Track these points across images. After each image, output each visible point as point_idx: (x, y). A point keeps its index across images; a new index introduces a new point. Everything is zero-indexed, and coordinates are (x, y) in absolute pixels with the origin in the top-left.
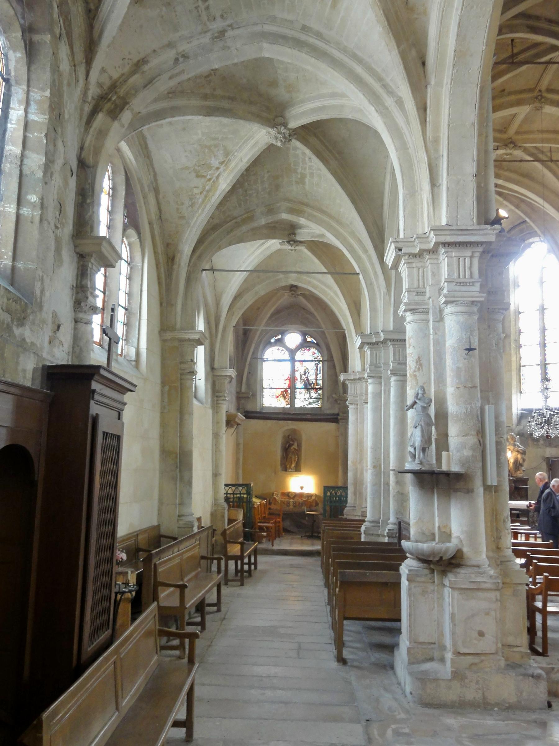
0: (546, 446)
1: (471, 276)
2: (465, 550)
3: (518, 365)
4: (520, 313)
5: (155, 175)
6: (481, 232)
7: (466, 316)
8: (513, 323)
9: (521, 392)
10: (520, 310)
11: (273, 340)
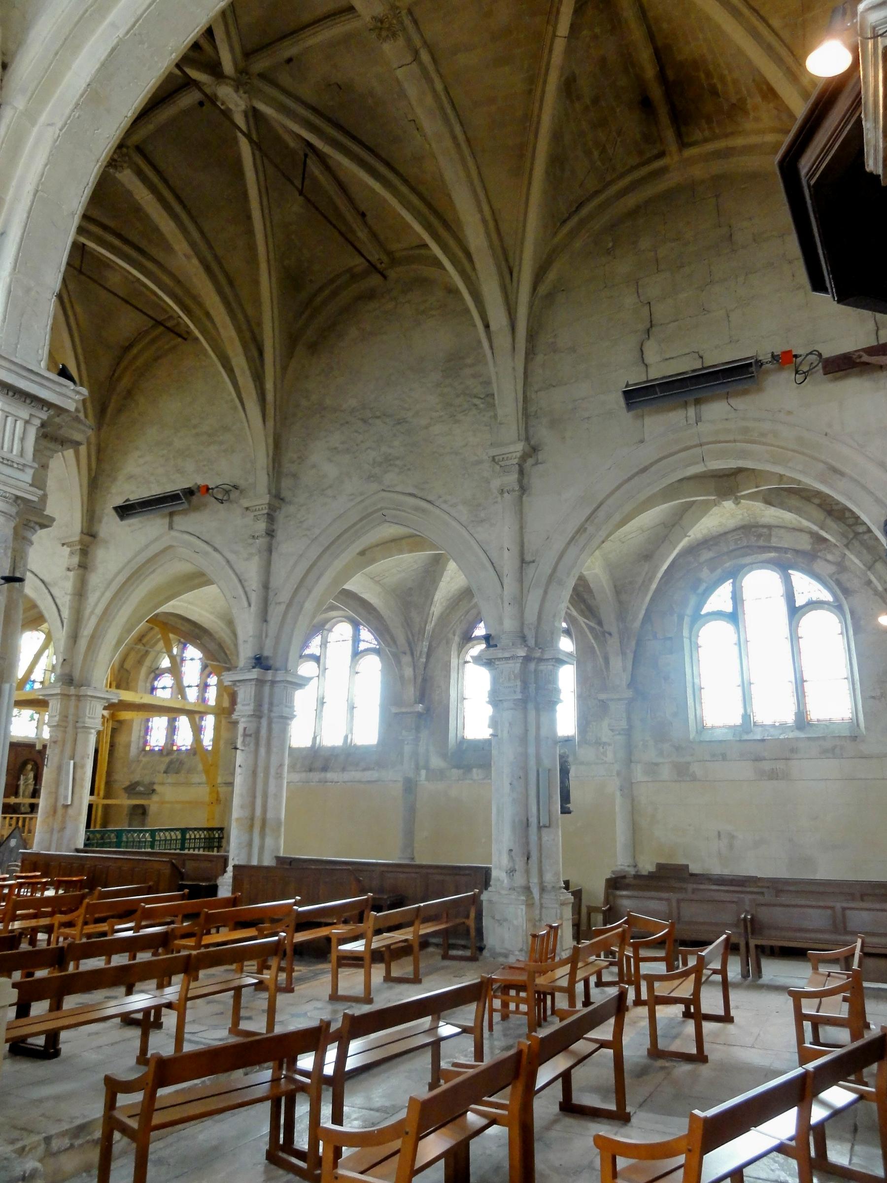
1: (22, 454)
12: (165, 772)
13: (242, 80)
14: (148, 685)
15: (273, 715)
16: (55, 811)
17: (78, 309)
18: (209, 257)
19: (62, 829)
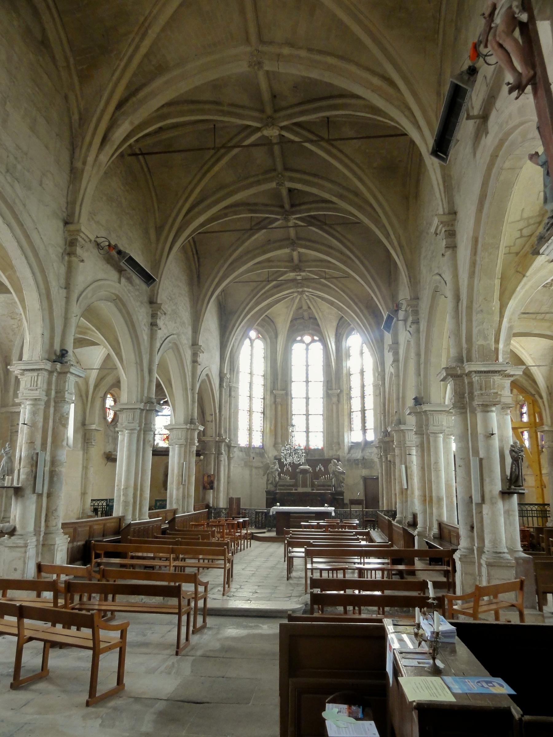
1: (37, 386)
2: (17, 527)
4: (350, 375)
6: (38, 364)
7: (32, 406)
8: (345, 382)
10: (351, 373)
11: (162, 402)
12: (528, 467)
13: (270, 122)
14: (518, 412)
15: (428, 431)
18: (341, 191)
19: (407, 501)
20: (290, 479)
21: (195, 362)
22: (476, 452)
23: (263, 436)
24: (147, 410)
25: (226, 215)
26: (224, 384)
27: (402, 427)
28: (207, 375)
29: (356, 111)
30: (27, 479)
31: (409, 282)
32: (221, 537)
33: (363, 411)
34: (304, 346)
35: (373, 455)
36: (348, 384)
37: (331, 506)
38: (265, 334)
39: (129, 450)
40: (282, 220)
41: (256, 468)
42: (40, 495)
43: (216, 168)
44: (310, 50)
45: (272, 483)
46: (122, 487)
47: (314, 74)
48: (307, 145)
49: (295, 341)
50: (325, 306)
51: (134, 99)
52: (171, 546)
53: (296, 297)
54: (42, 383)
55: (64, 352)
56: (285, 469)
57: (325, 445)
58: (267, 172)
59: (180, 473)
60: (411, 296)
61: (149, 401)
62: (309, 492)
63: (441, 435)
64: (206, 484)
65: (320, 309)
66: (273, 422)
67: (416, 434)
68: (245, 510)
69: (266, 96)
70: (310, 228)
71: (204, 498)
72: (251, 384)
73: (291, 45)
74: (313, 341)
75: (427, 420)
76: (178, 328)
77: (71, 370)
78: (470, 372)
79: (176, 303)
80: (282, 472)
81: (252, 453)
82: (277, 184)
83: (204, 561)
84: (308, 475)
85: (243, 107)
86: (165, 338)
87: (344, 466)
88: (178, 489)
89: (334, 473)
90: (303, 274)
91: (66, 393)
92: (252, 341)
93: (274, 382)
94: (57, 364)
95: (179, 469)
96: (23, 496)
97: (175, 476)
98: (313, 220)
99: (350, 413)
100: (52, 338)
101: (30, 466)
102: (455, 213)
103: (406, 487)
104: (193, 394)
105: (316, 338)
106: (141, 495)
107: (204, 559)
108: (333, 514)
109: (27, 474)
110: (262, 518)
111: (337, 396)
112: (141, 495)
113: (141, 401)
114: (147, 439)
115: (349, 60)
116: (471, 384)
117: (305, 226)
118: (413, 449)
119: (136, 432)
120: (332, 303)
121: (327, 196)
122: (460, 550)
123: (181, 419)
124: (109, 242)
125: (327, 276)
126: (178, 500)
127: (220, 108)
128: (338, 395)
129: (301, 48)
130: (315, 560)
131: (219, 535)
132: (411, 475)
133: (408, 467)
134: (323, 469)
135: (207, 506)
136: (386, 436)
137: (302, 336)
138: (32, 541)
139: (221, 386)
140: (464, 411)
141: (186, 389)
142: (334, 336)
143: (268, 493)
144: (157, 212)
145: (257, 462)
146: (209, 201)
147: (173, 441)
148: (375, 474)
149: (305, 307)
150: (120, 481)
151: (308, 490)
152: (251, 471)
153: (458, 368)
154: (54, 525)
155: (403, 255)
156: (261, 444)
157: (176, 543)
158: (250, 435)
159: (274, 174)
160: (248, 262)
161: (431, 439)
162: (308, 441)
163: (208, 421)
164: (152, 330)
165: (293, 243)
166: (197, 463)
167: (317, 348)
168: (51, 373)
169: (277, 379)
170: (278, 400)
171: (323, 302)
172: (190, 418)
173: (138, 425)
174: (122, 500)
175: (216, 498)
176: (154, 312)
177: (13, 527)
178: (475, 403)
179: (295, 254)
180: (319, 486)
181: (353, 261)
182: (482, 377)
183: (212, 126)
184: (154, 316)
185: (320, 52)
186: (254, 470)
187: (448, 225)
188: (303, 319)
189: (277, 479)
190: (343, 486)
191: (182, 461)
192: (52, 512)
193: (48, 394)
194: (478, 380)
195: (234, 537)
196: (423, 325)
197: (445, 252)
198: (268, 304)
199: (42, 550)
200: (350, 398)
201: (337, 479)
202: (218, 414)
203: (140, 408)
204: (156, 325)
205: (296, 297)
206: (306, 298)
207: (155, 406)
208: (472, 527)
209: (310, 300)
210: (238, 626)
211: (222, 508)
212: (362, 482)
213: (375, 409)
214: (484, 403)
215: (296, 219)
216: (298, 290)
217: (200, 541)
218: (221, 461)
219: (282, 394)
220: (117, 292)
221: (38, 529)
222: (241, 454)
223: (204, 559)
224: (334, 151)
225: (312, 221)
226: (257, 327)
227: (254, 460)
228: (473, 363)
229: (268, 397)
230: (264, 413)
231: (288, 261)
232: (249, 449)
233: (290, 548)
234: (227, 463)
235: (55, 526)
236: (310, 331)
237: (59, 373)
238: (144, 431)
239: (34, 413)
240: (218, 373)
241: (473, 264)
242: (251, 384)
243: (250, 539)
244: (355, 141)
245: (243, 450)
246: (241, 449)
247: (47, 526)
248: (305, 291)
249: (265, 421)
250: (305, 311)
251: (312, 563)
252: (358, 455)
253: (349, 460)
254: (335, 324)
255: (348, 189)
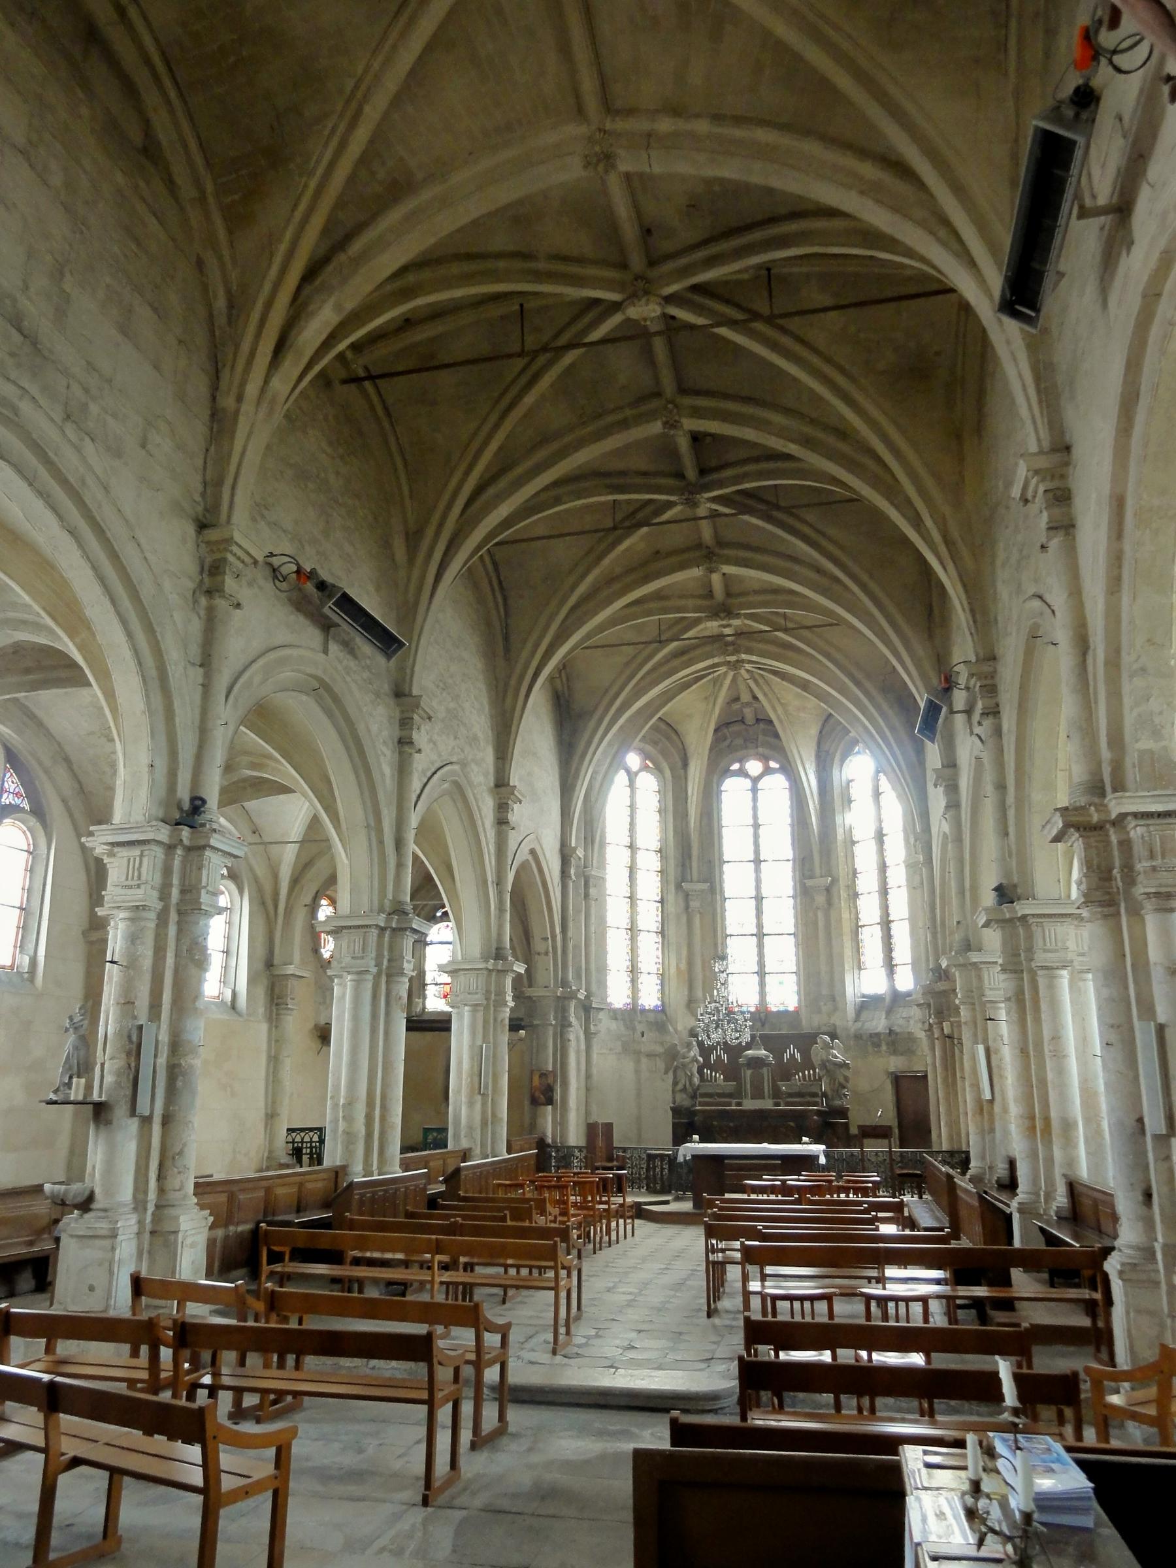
0: (891, 1054)
1: (139, 878)
2: (97, 1191)
3: (853, 925)
4: (854, 843)
5: (59, 744)
6: (141, 830)
7: (128, 923)
8: (841, 859)
9: (860, 968)
11: (439, 914)
13: (640, 287)
15: (1033, 965)
16: (982, 1110)
17: (832, 531)
18: (808, 430)
19: (992, 1130)
20: (725, 1080)
21: (502, 822)
22: (1148, 1010)
23: (662, 985)
24: (394, 930)
25: (558, 501)
26: (572, 871)
27: (975, 957)
28: (533, 852)
29: (826, 245)
30: (118, 1084)
31: (971, 623)
32: (562, 1214)
33: (886, 924)
34: (748, 783)
35: (912, 1022)
36: (850, 865)
37: (817, 1141)
38: (661, 758)
39: (355, 1018)
40: (682, 504)
41: (650, 1055)
42: (146, 1121)
43: (529, 399)
44: (717, 118)
45: (684, 1090)
46: (342, 1101)
47: (730, 170)
48: (723, 331)
49: (727, 773)
50: (789, 693)
51: (342, 257)
52: (434, 1237)
53: (725, 674)
54: (151, 873)
55: (198, 803)
56: (713, 1057)
57: (803, 1004)
58: (641, 399)
59: (476, 1069)
60: (977, 656)
61: (398, 910)
62: (771, 1110)
63: (1065, 973)
64: (537, 1094)
65: (778, 699)
66: (684, 953)
67: (1004, 970)
68: (625, 1150)
69: (630, 232)
70: (746, 517)
71: (533, 1126)
72: (632, 869)
73: (676, 111)
74: (767, 771)
75: (1030, 937)
76: (462, 751)
77: (213, 842)
78: (1123, 816)
79: (458, 696)
80: (707, 1064)
81: (640, 1022)
82: (665, 424)
83: (518, 1272)
84: (765, 1070)
85: (580, 261)
86: (433, 770)
87: (846, 1050)
88: (471, 1104)
89: (823, 1065)
90: (736, 622)
91: (203, 892)
92: (632, 776)
93: (683, 865)
94: (182, 830)
95: (472, 1058)
96: (108, 1123)
97: (464, 1076)
98: (750, 502)
99: (857, 928)
100: (172, 774)
101: (124, 1056)
102: (1068, 449)
103: (988, 1096)
104: (500, 893)
105: (773, 765)
106: (383, 1119)
107: (518, 1267)
108: (823, 1160)
109: (118, 1074)
110: (662, 1169)
111: (825, 893)
112: (383, 1119)
113: (381, 910)
114: (394, 993)
115: (807, 132)
116: (1126, 845)
117: (732, 515)
118: (1000, 1008)
119: (370, 977)
120: (805, 686)
121: (775, 443)
122: (1120, 1250)
123: (476, 950)
124: (298, 564)
125: (790, 625)
126: (470, 1128)
127: (533, 265)
128: (828, 890)
129: (698, 116)
130: (769, 1270)
131: (556, 1211)
132: (999, 1067)
133: (992, 1049)
134: (798, 1056)
135: (541, 1144)
136: (940, 979)
137: (741, 761)
138: (128, 1225)
139: (564, 874)
140: (1112, 910)
141: (485, 882)
142: (813, 758)
143: (676, 1111)
144: (407, 501)
145: (650, 1043)
146: (519, 470)
147: (459, 999)
148: (918, 1067)
149: (745, 697)
150: (337, 1087)
151: (767, 1104)
152: (638, 1062)
153: (1092, 808)
154: (178, 1188)
155: (954, 562)
156: (659, 1003)
157: (452, 1230)
158: (634, 982)
159: (654, 404)
160: (611, 603)
161: (1042, 982)
162: (763, 993)
163: (539, 954)
164: (401, 753)
165: (709, 555)
166: (511, 1045)
167: (776, 787)
168: (170, 848)
169: (690, 857)
170: (695, 904)
171: (784, 683)
172: (494, 946)
173: (373, 963)
174: (341, 1129)
175: (561, 1123)
176: (406, 715)
177: (87, 1193)
178: (1139, 890)
179: (716, 578)
180: (790, 1095)
181: (846, 587)
182: (1152, 828)
183: (517, 307)
184: (405, 723)
185: (739, 120)
186: (644, 1060)
187: (1053, 477)
188: (743, 722)
189: (696, 1080)
190: (846, 1096)
191: (479, 1042)
192: (173, 1158)
193: (164, 895)
194: (1143, 837)
195: (592, 1213)
196: (1008, 721)
197: (1049, 539)
198: (664, 693)
199: (151, 1244)
200: (856, 895)
201: (833, 1079)
202: (559, 938)
203: (377, 926)
204: (411, 743)
205: (725, 674)
206: (746, 676)
207: (411, 921)
208: (1148, 1196)
209: (756, 681)
210: (583, 1431)
211: (575, 1147)
212: (889, 1088)
213: (912, 920)
214: (1163, 890)
215: (714, 500)
216: (729, 658)
217: (509, 1223)
218: (569, 1040)
219: (703, 891)
220: (319, 673)
221: (141, 1196)
222: (613, 1025)
223: (518, 1267)
224: (785, 341)
225: (747, 502)
226: (642, 745)
227: (644, 1039)
228: (1127, 794)
229: (671, 898)
230: (662, 933)
231: (700, 597)
232: (633, 1013)
233: (714, 1242)
234: (583, 1047)
235: (179, 1190)
236: (760, 750)
237: (189, 849)
238: (389, 976)
239: (133, 939)
240: (557, 846)
241: (1116, 560)
242: (632, 869)
243: (632, 1218)
244: (833, 314)
245: (619, 1017)
246: (615, 1014)
247: (161, 1191)
248: (743, 661)
249: (666, 952)
250: (748, 704)
251: (764, 1277)
252: (878, 1023)
253: (858, 1037)
254: (814, 731)
255: (826, 428)
